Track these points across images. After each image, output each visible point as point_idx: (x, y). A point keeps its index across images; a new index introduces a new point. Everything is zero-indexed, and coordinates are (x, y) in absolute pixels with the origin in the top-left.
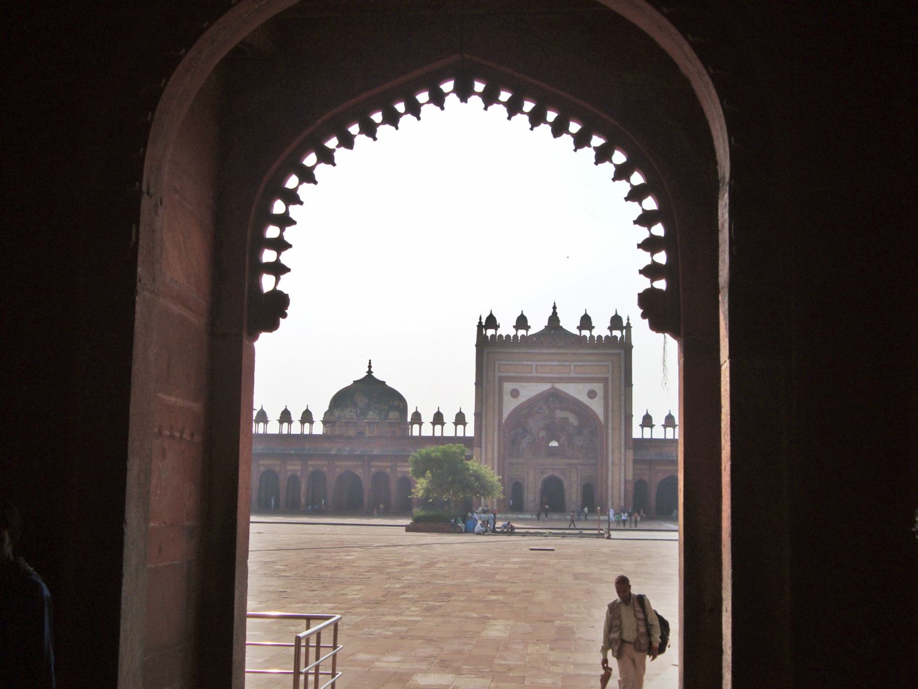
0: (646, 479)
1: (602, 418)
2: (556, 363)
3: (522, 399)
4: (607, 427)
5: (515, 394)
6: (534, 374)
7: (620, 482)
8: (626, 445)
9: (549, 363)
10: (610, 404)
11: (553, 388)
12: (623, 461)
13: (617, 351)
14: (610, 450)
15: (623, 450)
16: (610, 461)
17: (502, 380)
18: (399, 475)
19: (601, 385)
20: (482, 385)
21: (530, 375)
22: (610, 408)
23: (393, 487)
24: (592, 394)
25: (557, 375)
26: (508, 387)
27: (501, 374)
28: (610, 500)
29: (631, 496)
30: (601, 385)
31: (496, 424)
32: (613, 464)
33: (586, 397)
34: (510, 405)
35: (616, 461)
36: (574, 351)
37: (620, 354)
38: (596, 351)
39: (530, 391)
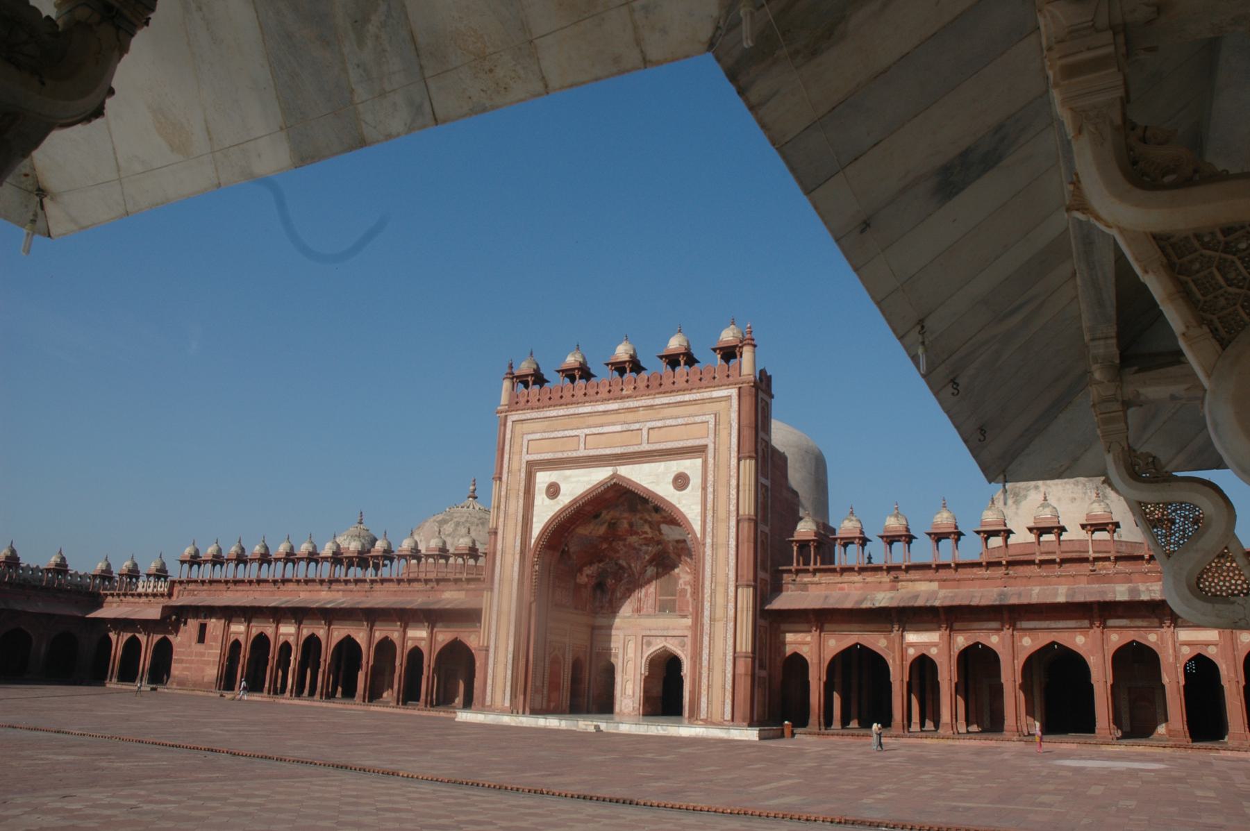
0: (805, 651)
1: (697, 527)
2: (618, 428)
3: (564, 499)
4: (704, 545)
5: (553, 491)
6: (582, 453)
7: (725, 655)
8: (737, 580)
9: (605, 429)
10: (710, 497)
11: (614, 476)
12: (731, 613)
13: (723, 393)
14: (707, 591)
15: (732, 589)
16: (707, 613)
17: (532, 468)
18: (410, 645)
19: (699, 462)
20: (500, 479)
21: (575, 454)
22: (710, 505)
23: (400, 662)
24: (681, 481)
25: (618, 451)
26: (543, 479)
27: (531, 458)
28: (704, 692)
29: (744, 685)
30: (699, 462)
31: (518, 549)
32: (712, 619)
33: (671, 487)
34: (545, 511)
35: (719, 613)
36: (649, 402)
37: (729, 397)
38: (687, 397)
39: (578, 484)
